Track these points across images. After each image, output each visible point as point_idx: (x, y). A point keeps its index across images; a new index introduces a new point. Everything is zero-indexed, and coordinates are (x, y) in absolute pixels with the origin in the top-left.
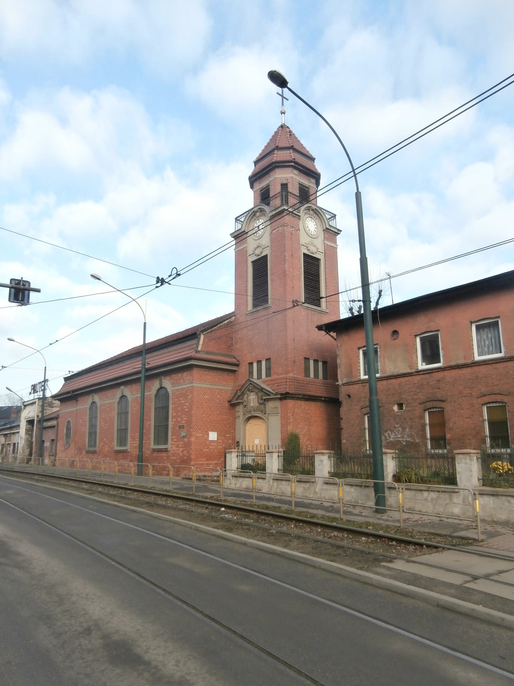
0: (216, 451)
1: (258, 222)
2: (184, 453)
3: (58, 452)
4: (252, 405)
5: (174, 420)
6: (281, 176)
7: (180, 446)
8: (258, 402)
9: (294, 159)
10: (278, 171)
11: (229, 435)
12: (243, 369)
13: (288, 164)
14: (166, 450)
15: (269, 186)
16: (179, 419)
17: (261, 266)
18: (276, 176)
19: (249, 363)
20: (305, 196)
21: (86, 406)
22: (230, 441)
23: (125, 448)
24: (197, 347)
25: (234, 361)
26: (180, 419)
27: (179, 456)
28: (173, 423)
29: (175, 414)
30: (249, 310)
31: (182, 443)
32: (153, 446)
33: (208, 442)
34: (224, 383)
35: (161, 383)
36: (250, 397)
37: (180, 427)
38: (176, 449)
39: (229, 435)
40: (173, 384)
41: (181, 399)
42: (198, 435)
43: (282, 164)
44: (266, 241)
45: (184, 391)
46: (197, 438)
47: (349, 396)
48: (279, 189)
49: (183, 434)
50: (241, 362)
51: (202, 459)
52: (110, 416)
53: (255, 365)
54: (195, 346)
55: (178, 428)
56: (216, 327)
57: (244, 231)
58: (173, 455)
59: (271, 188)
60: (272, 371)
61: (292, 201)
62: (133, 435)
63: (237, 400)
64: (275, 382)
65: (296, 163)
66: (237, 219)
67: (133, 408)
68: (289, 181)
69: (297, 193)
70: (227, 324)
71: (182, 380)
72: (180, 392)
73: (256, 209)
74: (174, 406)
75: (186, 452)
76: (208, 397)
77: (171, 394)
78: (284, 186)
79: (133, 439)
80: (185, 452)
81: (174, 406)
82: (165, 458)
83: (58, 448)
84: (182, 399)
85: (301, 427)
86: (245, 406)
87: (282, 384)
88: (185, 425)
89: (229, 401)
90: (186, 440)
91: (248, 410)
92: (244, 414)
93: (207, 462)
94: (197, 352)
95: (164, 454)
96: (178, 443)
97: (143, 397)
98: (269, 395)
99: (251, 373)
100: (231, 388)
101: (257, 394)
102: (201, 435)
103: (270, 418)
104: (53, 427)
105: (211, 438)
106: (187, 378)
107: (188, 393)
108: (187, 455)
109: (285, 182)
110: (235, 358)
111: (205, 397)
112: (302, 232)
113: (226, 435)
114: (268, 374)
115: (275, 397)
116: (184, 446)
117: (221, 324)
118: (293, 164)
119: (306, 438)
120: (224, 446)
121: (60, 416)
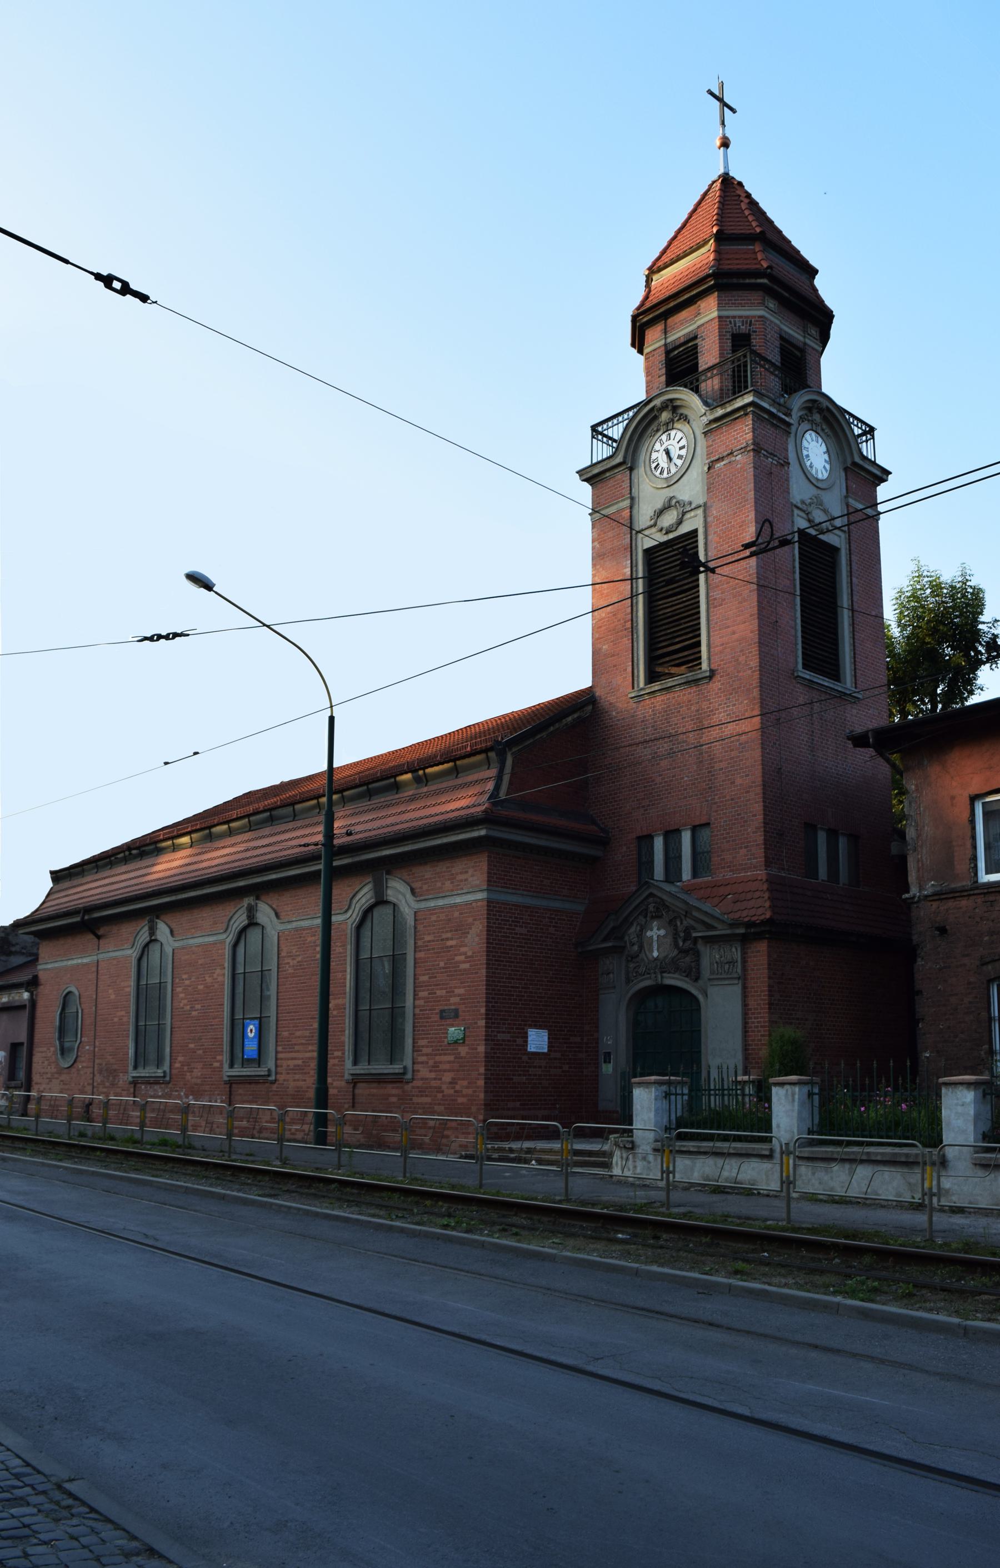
1: (664, 437)
4: (655, 954)
8: (676, 945)
11: (578, 1039)
13: (753, 281)
16: (439, 993)
26: (439, 993)
27: (440, 1096)
31: (451, 1058)
33: (525, 1058)
36: (649, 934)
37: (443, 1015)
38: (433, 1075)
39: (578, 1039)
41: (444, 936)
42: (500, 1036)
43: (735, 281)
47: (943, 930)
49: (454, 1032)
52: (209, 980)
53: (659, 843)
55: (437, 1018)
56: (544, 734)
63: (605, 940)
65: (771, 277)
69: (775, 357)
71: (448, 884)
72: (442, 917)
73: (657, 402)
75: (465, 1083)
76: (524, 931)
82: (394, 1099)
84: (449, 935)
86: (633, 958)
87: (749, 896)
88: (462, 1008)
90: (463, 1050)
92: (628, 981)
95: (392, 1090)
96: (438, 1058)
98: (714, 928)
101: (671, 922)
102: (507, 1037)
103: (712, 991)
105: (532, 1048)
107: (470, 920)
108: (470, 1091)
109: (744, 329)
111: (518, 930)
112: (794, 468)
115: (728, 932)
117: (557, 725)
118: (765, 281)
120: (566, 1067)
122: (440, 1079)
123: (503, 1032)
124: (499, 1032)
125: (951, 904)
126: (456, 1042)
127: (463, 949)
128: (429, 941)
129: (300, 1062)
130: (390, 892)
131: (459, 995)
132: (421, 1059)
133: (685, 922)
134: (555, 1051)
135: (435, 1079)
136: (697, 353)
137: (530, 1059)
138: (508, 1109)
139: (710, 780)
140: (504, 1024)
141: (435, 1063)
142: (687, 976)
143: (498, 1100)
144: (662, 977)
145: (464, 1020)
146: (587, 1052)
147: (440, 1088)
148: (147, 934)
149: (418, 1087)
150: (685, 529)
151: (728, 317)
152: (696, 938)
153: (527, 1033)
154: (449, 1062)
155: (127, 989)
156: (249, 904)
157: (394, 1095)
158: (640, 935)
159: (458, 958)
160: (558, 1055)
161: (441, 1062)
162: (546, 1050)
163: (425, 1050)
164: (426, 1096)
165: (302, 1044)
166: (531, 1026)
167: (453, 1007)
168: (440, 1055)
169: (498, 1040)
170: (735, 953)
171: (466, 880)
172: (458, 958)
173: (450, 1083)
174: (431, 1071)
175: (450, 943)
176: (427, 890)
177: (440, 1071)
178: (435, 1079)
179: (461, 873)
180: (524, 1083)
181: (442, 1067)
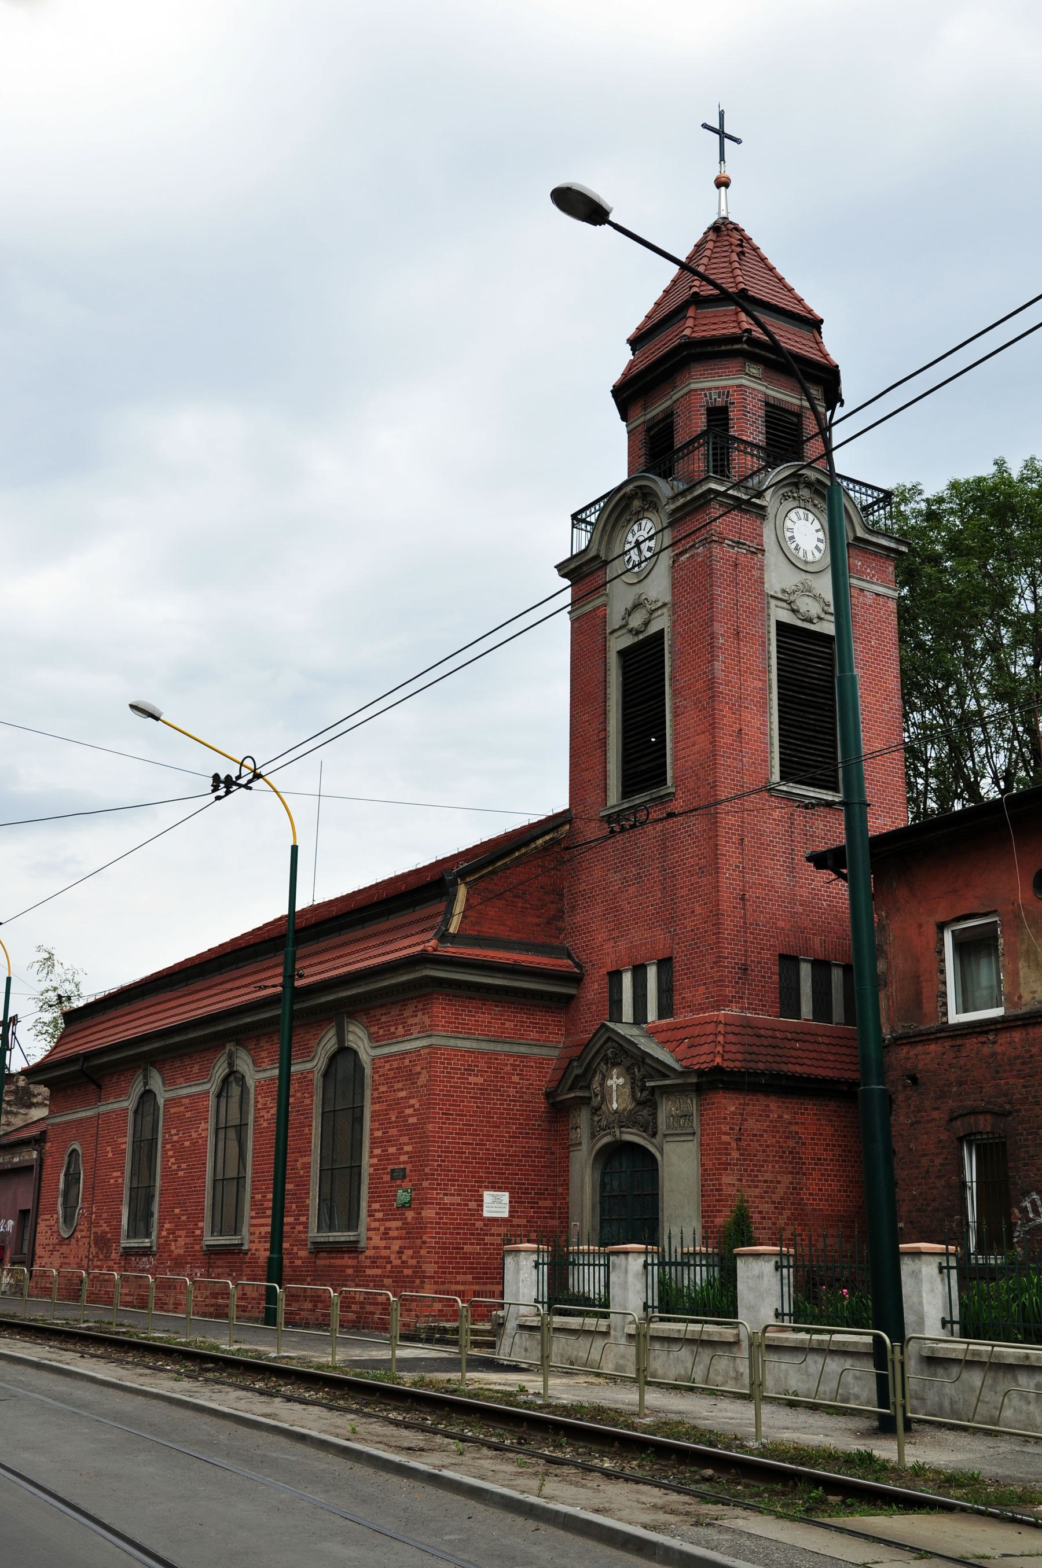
2: (404, 1258)
3: (39, 1251)
4: (615, 1106)
6: (708, 384)
7: (393, 1233)
10: (696, 369)
11: (549, 1203)
12: (594, 989)
13: (729, 347)
14: (352, 1248)
15: (672, 414)
16: (392, 1150)
18: (693, 386)
19: (610, 974)
21: (125, 1104)
22: (551, 1222)
23: (235, 1240)
24: (447, 922)
25: (564, 964)
26: (392, 1150)
28: (375, 1161)
29: (379, 1134)
31: (399, 1224)
32: (314, 1233)
33: (479, 1224)
34: (534, 1035)
35: (341, 1036)
36: (609, 1082)
38: (383, 1243)
39: (549, 1203)
40: (375, 1039)
42: (447, 1200)
43: (709, 349)
44: (658, 587)
46: (444, 1208)
47: (914, 1080)
48: (700, 423)
49: (403, 1196)
50: (588, 967)
51: (460, 1278)
52: (194, 1135)
53: (627, 979)
54: (440, 919)
55: (387, 1178)
57: (597, 557)
58: (374, 1262)
59: (679, 422)
60: (677, 998)
61: (742, 462)
62: (259, 1197)
63: (571, 1089)
64: (681, 1034)
66: (577, 518)
67: (261, 1112)
68: (731, 399)
70: (546, 848)
72: (395, 1065)
74: (377, 1107)
77: (368, 1071)
81: (377, 1107)
82: (350, 1271)
83: (41, 1239)
84: (400, 1085)
85: (768, 1176)
87: (703, 1040)
88: (409, 1167)
90: (410, 1215)
91: (604, 1123)
92: (593, 1136)
93: (476, 1288)
94: (444, 937)
95: (347, 1261)
96: (388, 1224)
97: (286, 1077)
98: (665, 1076)
99: (616, 1003)
100: (556, 1053)
101: (629, 1070)
102: (457, 1199)
103: (667, 1147)
104: (24, 1170)
107: (418, 1069)
108: (413, 1262)
109: (720, 402)
110: (570, 957)
111: (472, 1079)
113: (541, 1203)
114: (664, 1011)
117: (523, 851)
119: (787, 1213)
121: (50, 1135)
122: (389, 1248)
123: (453, 1195)
124: (446, 1195)
125: (920, 1048)
126: (403, 1206)
127: (412, 1102)
128: (383, 1092)
130: (351, 1037)
133: (642, 1070)
134: (519, 1217)
135: (385, 1248)
136: (673, 431)
137: (485, 1225)
138: (457, 1283)
139: (673, 909)
140: (453, 1185)
141: (385, 1229)
142: (644, 1131)
143: (444, 1273)
144: (621, 1132)
146: (559, 1218)
147: (389, 1257)
149: (370, 1257)
151: (703, 390)
152: (653, 1087)
153: (482, 1196)
155: (123, 1146)
158: (602, 1084)
161: (390, 1229)
162: (506, 1215)
164: (377, 1267)
166: (487, 1188)
167: (402, 1166)
168: (390, 1220)
169: (445, 1204)
170: (691, 1105)
173: (398, 1252)
174: (381, 1239)
176: (383, 1035)
177: (389, 1238)
178: (385, 1248)
180: (478, 1253)
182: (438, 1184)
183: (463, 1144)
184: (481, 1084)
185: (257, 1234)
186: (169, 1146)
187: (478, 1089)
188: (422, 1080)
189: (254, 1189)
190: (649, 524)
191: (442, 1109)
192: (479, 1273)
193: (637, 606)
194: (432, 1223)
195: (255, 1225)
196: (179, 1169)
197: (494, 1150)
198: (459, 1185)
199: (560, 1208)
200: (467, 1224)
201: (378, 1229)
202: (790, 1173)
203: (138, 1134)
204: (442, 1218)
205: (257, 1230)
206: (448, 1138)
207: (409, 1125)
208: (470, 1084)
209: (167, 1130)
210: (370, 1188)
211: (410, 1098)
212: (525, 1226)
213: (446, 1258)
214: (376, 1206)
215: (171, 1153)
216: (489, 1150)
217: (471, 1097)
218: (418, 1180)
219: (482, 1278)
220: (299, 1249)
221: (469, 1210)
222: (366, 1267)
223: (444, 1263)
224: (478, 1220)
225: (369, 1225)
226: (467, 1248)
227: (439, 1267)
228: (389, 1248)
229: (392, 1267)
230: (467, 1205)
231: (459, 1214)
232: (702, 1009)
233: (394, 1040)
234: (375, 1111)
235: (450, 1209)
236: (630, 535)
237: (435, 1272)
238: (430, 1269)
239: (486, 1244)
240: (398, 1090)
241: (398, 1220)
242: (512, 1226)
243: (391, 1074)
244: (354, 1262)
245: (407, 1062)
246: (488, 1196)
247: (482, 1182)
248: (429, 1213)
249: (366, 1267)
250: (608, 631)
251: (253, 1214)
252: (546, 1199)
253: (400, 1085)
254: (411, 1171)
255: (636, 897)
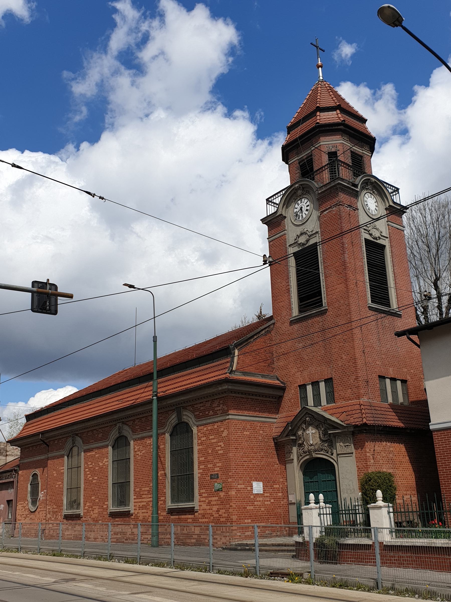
0: (263, 509)
1: (299, 202)
2: (220, 513)
4: (311, 442)
5: (202, 467)
6: (328, 143)
9: (344, 121)
13: (336, 127)
14: (191, 511)
15: (312, 155)
16: (209, 466)
17: (307, 258)
18: (321, 143)
20: (359, 165)
26: (209, 466)
28: (201, 471)
29: (203, 459)
30: (294, 315)
31: (217, 498)
32: (170, 504)
33: (252, 497)
35: (179, 416)
36: (307, 432)
37: (212, 477)
38: (208, 507)
43: (328, 128)
44: (313, 225)
45: (216, 427)
46: (238, 490)
48: (325, 159)
49: (217, 486)
50: (288, 384)
51: (246, 521)
52: (101, 464)
53: (309, 388)
57: (281, 215)
58: (203, 516)
59: (315, 158)
60: (336, 394)
64: (341, 410)
68: (338, 148)
69: (349, 161)
74: (201, 447)
78: (333, 155)
79: (139, 495)
80: (222, 512)
81: (201, 447)
84: (213, 437)
87: (354, 412)
89: (274, 439)
90: (222, 494)
96: (210, 499)
99: (304, 398)
102: (243, 486)
106: (218, 408)
107: (222, 429)
109: (333, 150)
111: (245, 433)
112: (361, 212)
113: (275, 486)
116: (219, 502)
118: (342, 127)
120: (272, 501)
122: (212, 509)
124: (238, 484)
126: (218, 490)
127: (219, 444)
128: (203, 440)
129: (145, 503)
131: (219, 467)
132: (202, 499)
134: (267, 493)
135: (209, 509)
136: (312, 162)
137: (254, 497)
138: (245, 523)
140: (241, 480)
145: (221, 479)
146: (282, 492)
147: (212, 513)
148: (71, 443)
149: (201, 514)
150: (311, 242)
152: (330, 433)
153: (252, 484)
154: (216, 501)
156: (119, 426)
157: (190, 518)
159: (217, 448)
160: (268, 495)
161: (211, 501)
162: (262, 492)
163: (204, 495)
164: (205, 518)
165: (146, 494)
167: (217, 473)
168: (211, 497)
169: (238, 488)
171: (219, 410)
172: (217, 448)
173: (217, 511)
174: (207, 505)
175: (213, 441)
176: (202, 416)
178: (209, 509)
179: (217, 407)
181: (212, 503)
182: (235, 480)
183: (244, 461)
184: (249, 435)
185: (137, 507)
186: (87, 470)
187: (248, 437)
188: (225, 434)
189: (135, 486)
190: (306, 201)
191: (235, 447)
192: (253, 518)
193: (302, 234)
194: (234, 497)
195: (136, 502)
196: (93, 479)
197: (255, 464)
198: (243, 480)
199: (282, 488)
200: (247, 497)
201: (205, 501)
202: (392, 468)
203: (70, 465)
204: (237, 495)
205: (137, 504)
206: (238, 459)
207: (219, 454)
208: (244, 435)
209: (86, 463)
210: (199, 483)
211: (218, 442)
212: (269, 497)
213: (240, 512)
214: (202, 491)
215: (88, 473)
216: (253, 464)
217: (246, 441)
218: (226, 478)
219: (255, 521)
220: (161, 512)
221: (248, 490)
222: (199, 518)
223: (240, 515)
224: (251, 495)
225: (200, 499)
226: (248, 508)
227: (238, 517)
228: (212, 509)
229: (214, 518)
230: (247, 489)
231: (244, 493)
232: (350, 399)
233: (208, 418)
234: (200, 449)
235: (240, 491)
236: (297, 205)
237: (237, 519)
238: (234, 518)
239: (255, 505)
240: (212, 439)
241: (215, 496)
242: (264, 497)
243: (207, 432)
244: (192, 516)
245: (216, 427)
246: (255, 484)
247: (252, 478)
248: (233, 493)
249: (199, 518)
250: (288, 245)
251: (135, 497)
252: (276, 484)
253: (213, 437)
254: (221, 475)
255: (311, 353)
